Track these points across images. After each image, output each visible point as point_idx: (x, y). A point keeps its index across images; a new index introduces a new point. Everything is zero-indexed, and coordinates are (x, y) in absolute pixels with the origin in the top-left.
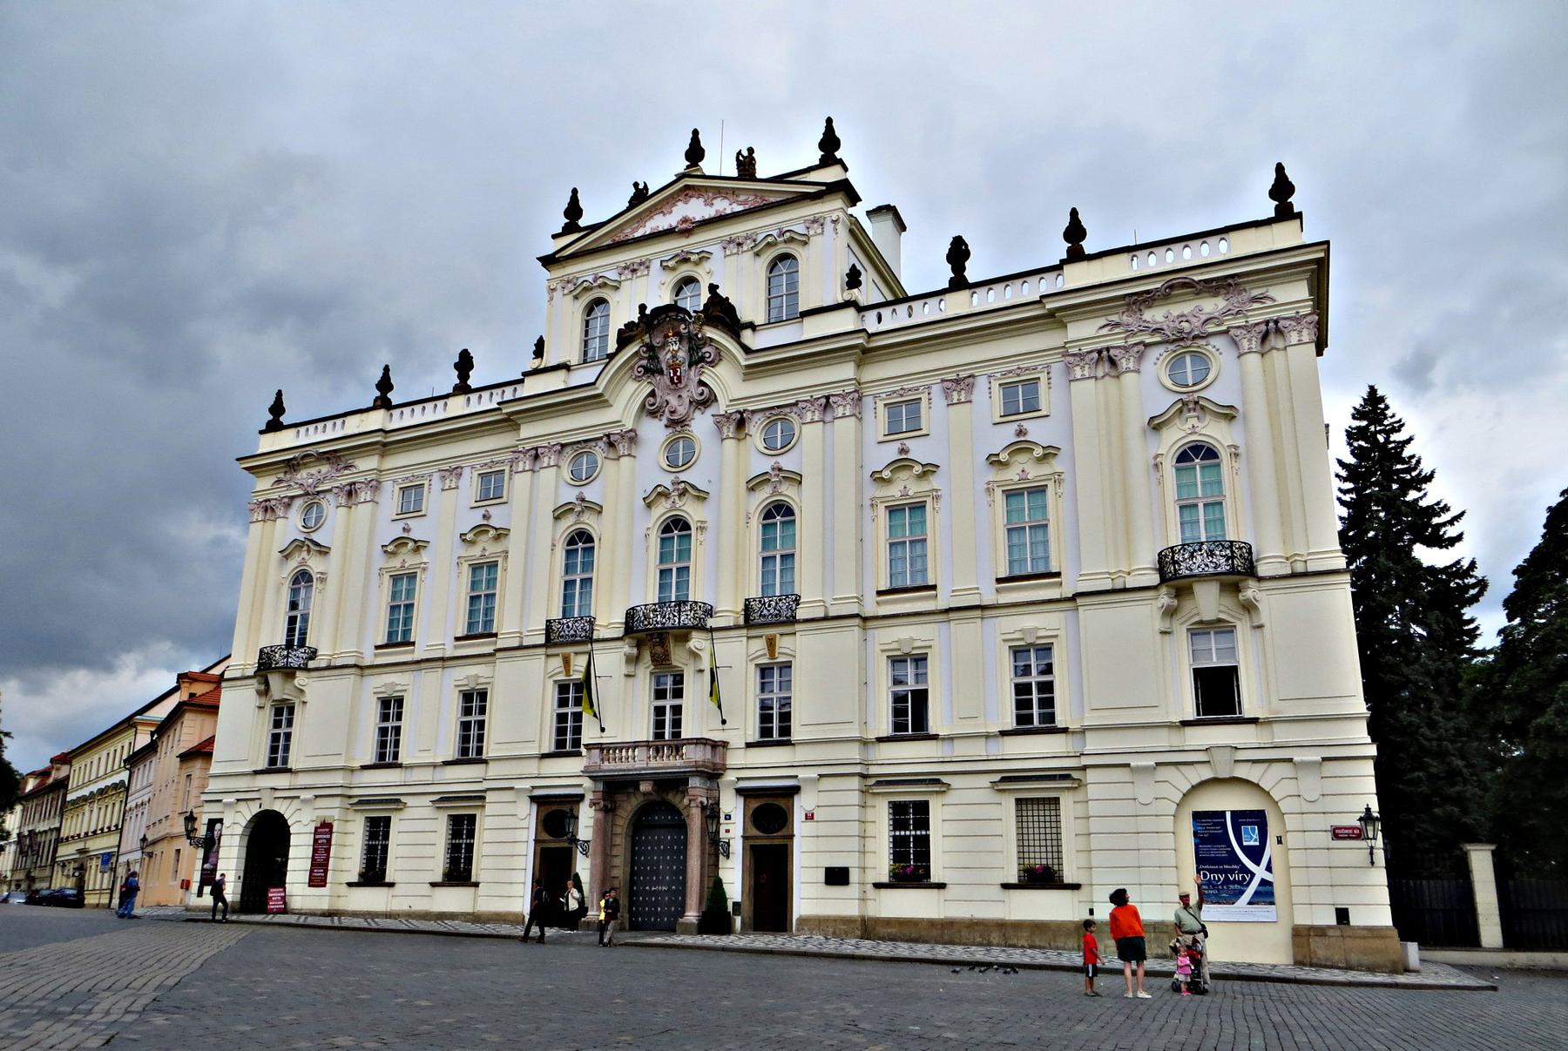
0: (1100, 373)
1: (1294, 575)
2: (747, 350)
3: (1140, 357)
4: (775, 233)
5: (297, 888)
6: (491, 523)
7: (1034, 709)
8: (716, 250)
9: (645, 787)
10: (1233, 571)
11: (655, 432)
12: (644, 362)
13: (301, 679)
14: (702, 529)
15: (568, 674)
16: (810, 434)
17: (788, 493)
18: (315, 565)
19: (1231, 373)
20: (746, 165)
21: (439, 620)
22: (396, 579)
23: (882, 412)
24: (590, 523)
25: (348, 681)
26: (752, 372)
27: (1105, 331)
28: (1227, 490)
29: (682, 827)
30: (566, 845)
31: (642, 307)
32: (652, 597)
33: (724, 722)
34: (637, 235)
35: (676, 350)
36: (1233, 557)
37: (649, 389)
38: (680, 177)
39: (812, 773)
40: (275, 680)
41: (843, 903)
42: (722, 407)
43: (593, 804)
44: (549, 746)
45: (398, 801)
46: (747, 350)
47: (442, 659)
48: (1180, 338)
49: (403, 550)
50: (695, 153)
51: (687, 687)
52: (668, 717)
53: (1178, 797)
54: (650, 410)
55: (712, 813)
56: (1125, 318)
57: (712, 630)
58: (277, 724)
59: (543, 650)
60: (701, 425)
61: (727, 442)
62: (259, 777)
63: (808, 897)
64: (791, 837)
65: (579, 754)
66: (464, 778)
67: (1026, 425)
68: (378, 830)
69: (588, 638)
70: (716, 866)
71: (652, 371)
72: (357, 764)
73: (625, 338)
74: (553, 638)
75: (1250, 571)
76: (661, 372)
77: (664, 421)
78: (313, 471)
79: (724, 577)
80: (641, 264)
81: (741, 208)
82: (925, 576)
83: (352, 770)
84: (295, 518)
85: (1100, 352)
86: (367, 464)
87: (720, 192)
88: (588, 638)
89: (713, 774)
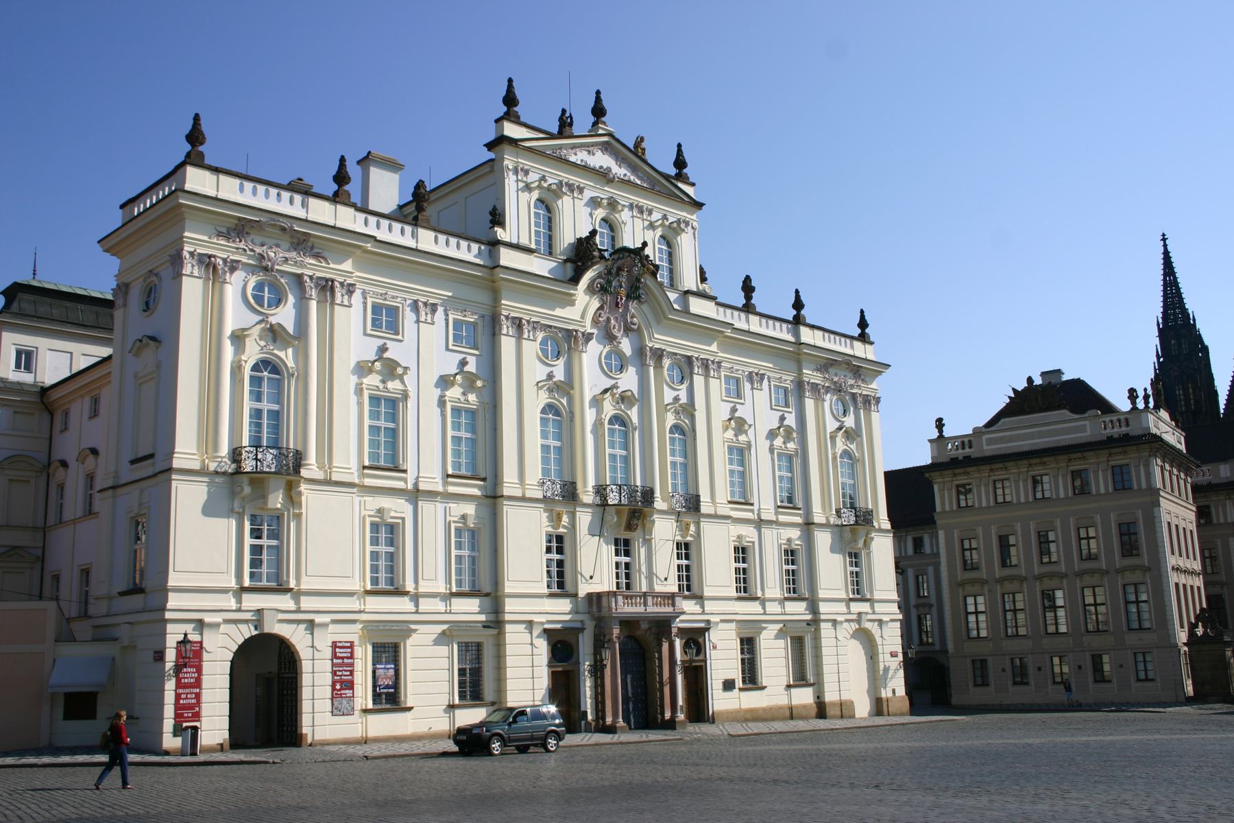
5: (319, 719)
9: (644, 626)
34: (572, 159)
50: (599, 111)
78: (270, 242)
81: (639, 182)
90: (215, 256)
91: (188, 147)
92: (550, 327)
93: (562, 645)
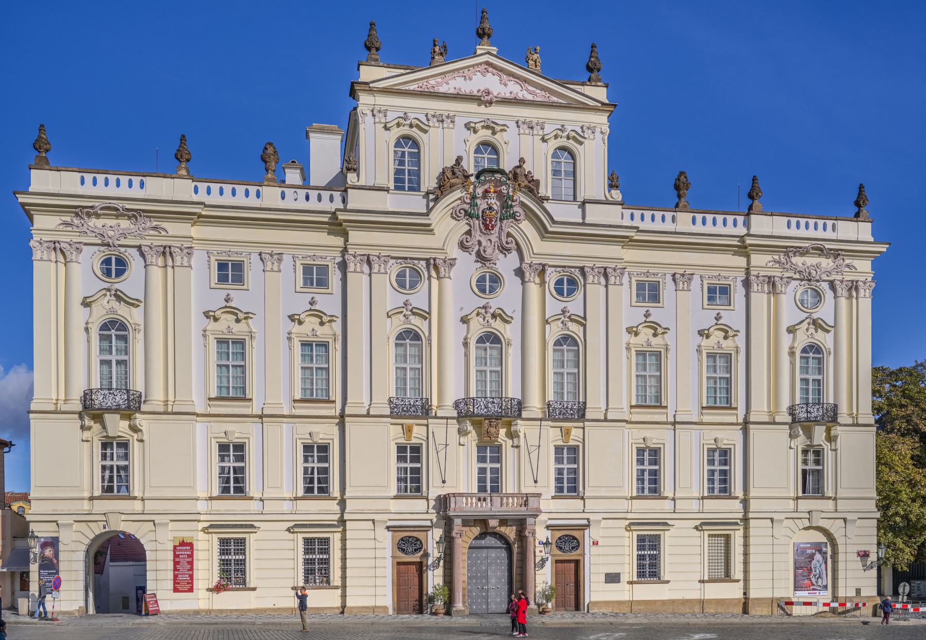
12: (466, 207)
15: (409, 438)
31: (459, 160)
59: (389, 420)
69: (425, 411)
88: (425, 411)
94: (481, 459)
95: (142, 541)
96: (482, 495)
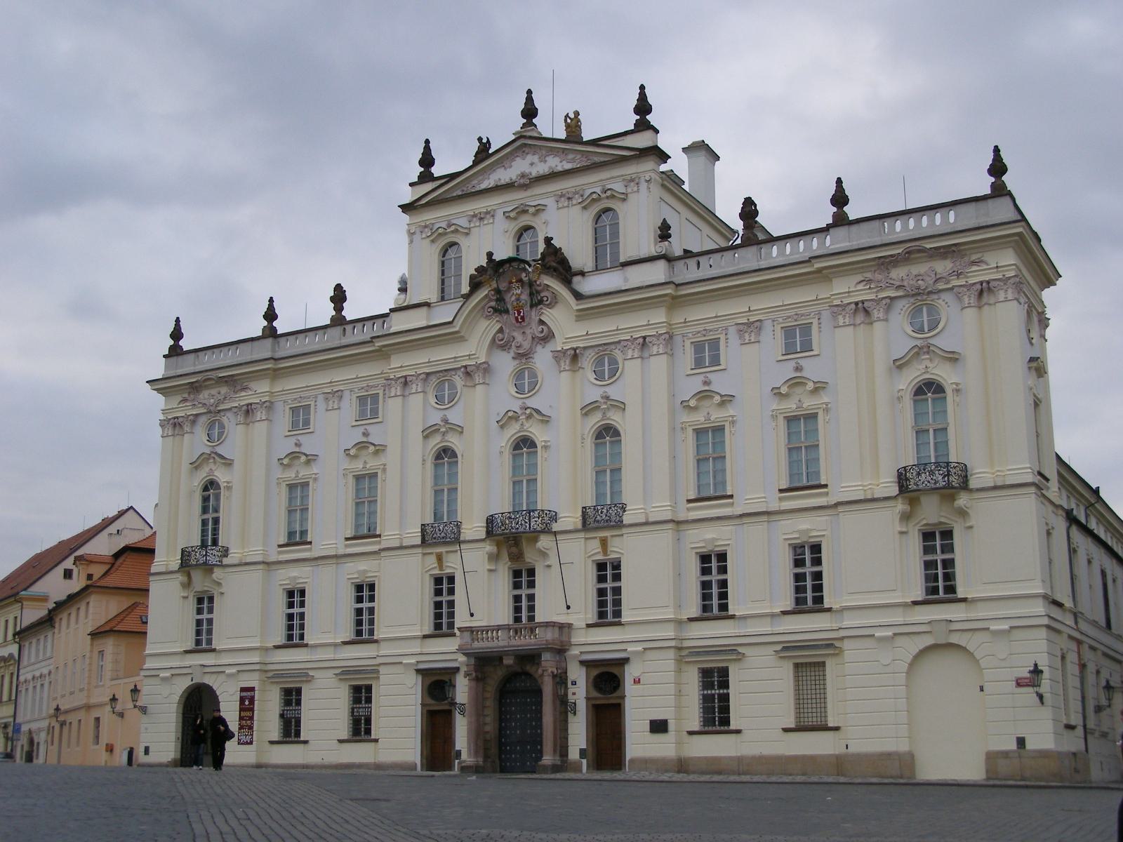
0: (858, 321)
1: (995, 488)
2: (578, 296)
3: (888, 308)
4: (598, 190)
6: (371, 439)
7: (809, 591)
8: (550, 202)
9: (508, 661)
10: (949, 486)
11: (505, 363)
12: (493, 304)
13: (218, 574)
14: (546, 447)
16: (631, 368)
17: (615, 418)
18: (221, 476)
19: (959, 325)
20: (573, 125)
21: (330, 523)
22: (291, 487)
23: (690, 350)
24: (454, 441)
25: (256, 575)
26: (582, 316)
27: (860, 287)
28: (951, 419)
29: (539, 692)
30: (447, 707)
31: (490, 255)
32: (507, 508)
33: (568, 607)
34: (483, 186)
35: (518, 294)
36: (948, 475)
37: (498, 327)
38: (520, 136)
39: (639, 648)
40: (197, 576)
41: (663, 747)
42: (558, 344)
43: (467, 675)
44: (428, 628)
45: (307, 675)
46: (578, 296)
47: (336, 556)
48: (917, 293)
49: (296, 462)
50: (530, 112)
51: (538, 578)
52: (524, 604)
53: (909, 658)
54: (500, 343)
55: (561, 679)
56: (878, 276)
57: (555, 533)
58: (199, 611)
59: (419, 550)
60: (542, 359)
61: (563, 374)
62: (189, 656)
63: (638, 743)
64: (623, 697)
65: (454, 635)
66: (360, 654)
67: (802, 362)
68: (292, 697)
69: (455, 539)
70: (566, 721)
71: (500, 310)
72: (270, 645)
73: (475, 285)
74: (428, 538)
75: (964, 486)
76: (507, 311)
77: (512, 354)
78: (214, 392)
79: (564, 488)
80: (488, 213)
81: (568, 166)
82: (725, 489)
83: (266, 650)
84: (200, 433)
85: (857, 304)
86: (261, 388)
87: (552, 151)
88: (455, 539)
89: (560, 651)
90: (177, 418)
91: (172, 342)
92: (441, 371)
93: (437, 685)
94: (517, 585)
95: (218, 693)
96: (518, 626)
